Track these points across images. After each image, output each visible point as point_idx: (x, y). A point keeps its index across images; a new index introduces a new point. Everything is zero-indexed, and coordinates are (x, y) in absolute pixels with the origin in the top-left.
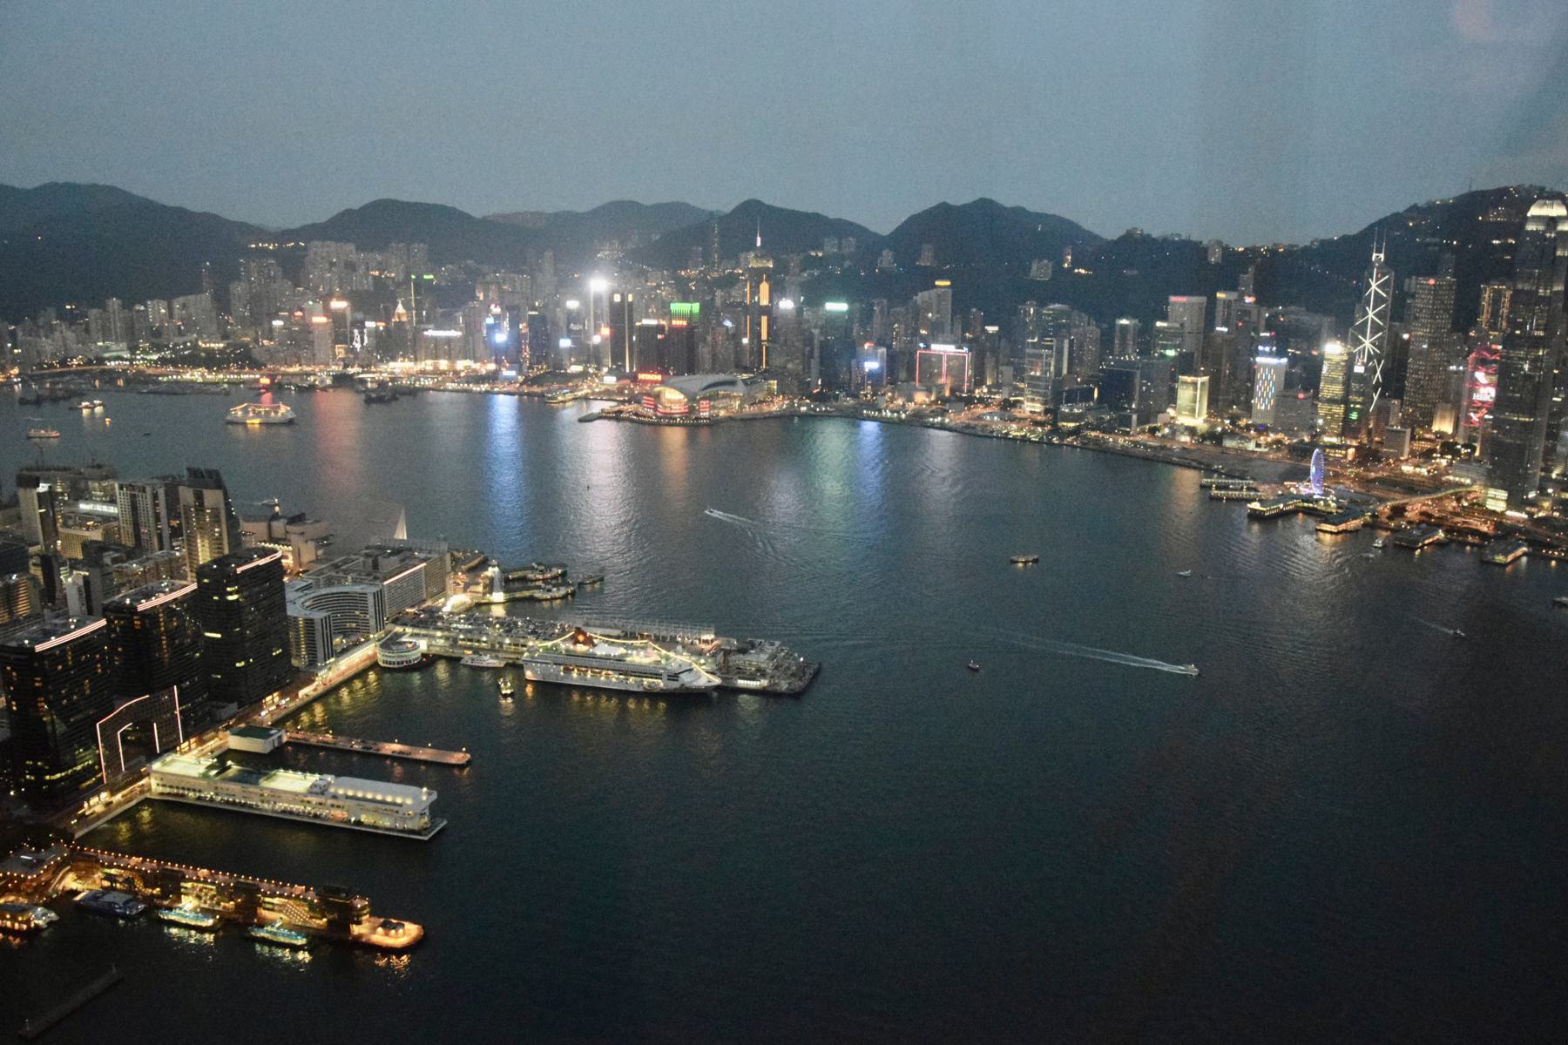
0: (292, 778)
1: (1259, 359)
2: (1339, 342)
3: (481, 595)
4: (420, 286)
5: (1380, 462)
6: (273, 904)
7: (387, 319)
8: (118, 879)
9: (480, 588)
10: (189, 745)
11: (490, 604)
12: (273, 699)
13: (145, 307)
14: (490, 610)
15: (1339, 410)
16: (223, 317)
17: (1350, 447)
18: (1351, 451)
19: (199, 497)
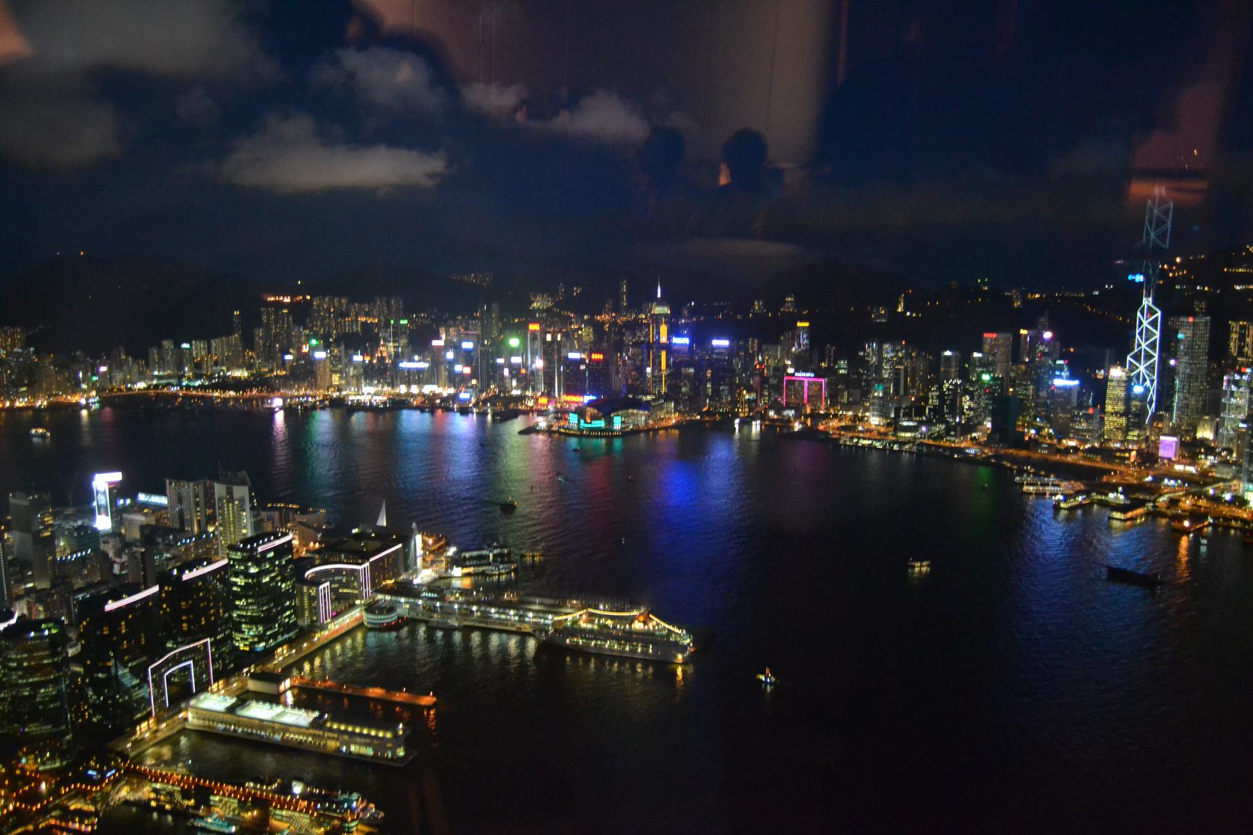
0: (299, 715)
1: (1058, 382)
2: (1119, 368)
3: (443, 570)
4: (397, 326)
5: (1157, 462)
6: (282, 816)
7: (372, 357)
8: (161, 792)
9: (444, 565)
10: (218, 686)
11: (451, 577)
12: (283, 650)
13: (191, 345)
14: (450, 583)
15: (1123, 421)
16: (248, 353)
17: (1133, 450)
18: (1134, 453)
19: (230, 492)
